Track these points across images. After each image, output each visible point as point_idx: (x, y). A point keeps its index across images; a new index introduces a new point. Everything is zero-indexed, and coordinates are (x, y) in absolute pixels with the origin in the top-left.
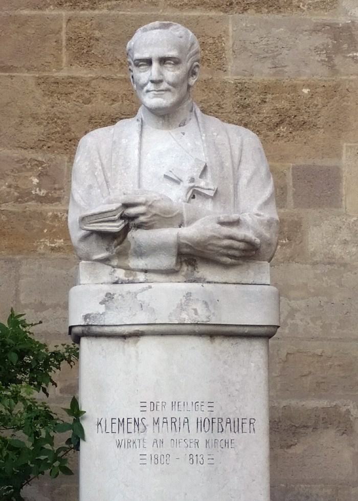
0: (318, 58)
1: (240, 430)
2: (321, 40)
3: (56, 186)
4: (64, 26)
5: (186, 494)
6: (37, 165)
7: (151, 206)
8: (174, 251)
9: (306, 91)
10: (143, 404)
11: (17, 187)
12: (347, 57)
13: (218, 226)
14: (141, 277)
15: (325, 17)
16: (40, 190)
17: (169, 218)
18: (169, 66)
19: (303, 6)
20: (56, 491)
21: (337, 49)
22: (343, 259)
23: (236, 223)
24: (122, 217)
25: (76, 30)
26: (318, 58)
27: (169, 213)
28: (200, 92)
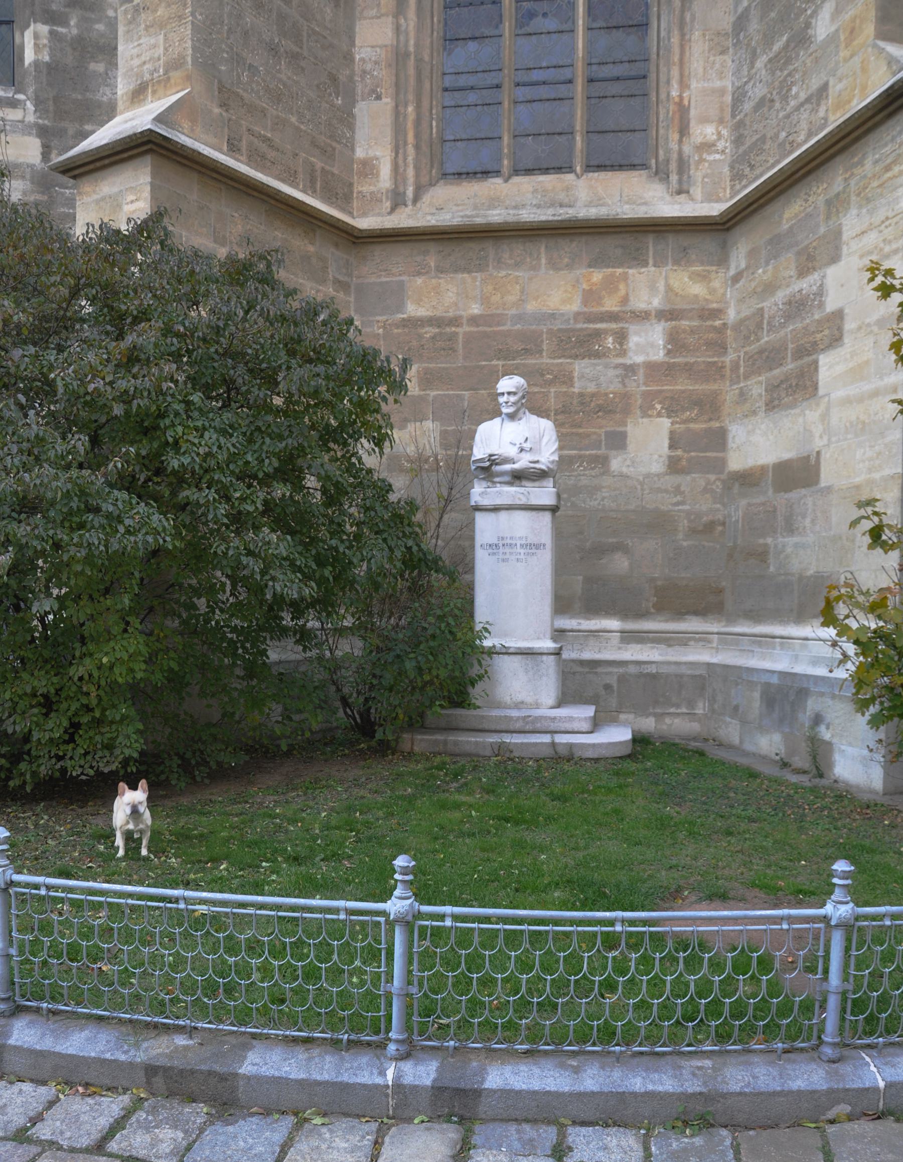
2: (619, 371)
15: (620, 361)
21: (626, 376)
23: (537, 462)
28: (531, 404)
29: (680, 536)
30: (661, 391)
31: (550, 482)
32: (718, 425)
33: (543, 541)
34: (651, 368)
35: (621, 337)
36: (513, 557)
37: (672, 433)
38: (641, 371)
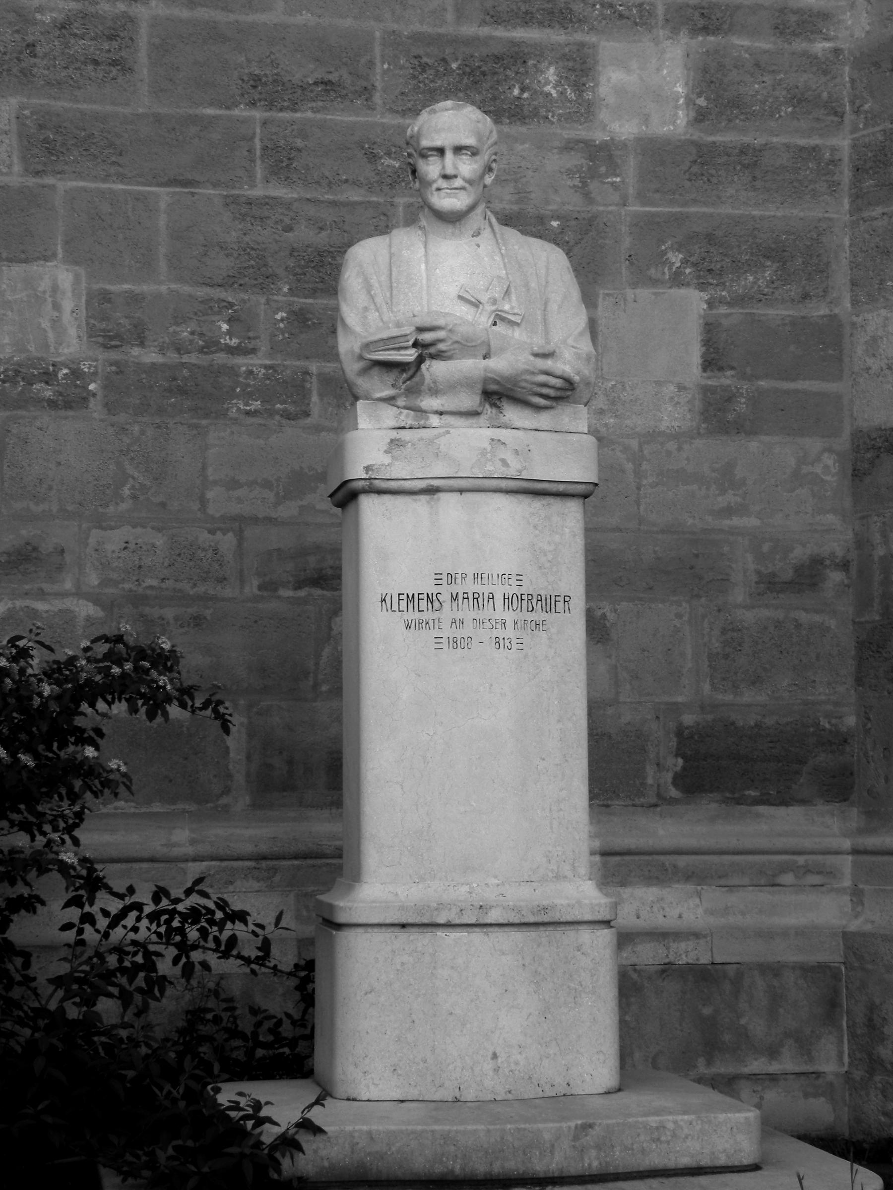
0: (569, 183)
1: (553, 610)
2: (575, 160)
3: (251, 334)
4: (258, 130)
5: (492, 685)
6: (226, 307)
7: (450, 331)
8: (479, 388)
9: (555, 224)
10: (438, 577)
11: (202, 335)
12: (605, 183)
13: (532, 358)
14: (434, 420)
15: (580, 132)
16: (231, 339)
17: (469, 346)
18: (464, 157)
19: (553, 116)
20: (255, 710)
21: (593, 174)
22: (599, 432)
24: (416, 344)
25: (274, 137)
26: (569, 183)
27: (472, 341)
29: (739, 595)
30: (679, 220)
31: (576, 418)
32: (824, 311)
33: (563, 589)
34: (655, 151)
35: (580, 69)
36: (486, 634)
37: (711, 331)
38: (631, 166)
